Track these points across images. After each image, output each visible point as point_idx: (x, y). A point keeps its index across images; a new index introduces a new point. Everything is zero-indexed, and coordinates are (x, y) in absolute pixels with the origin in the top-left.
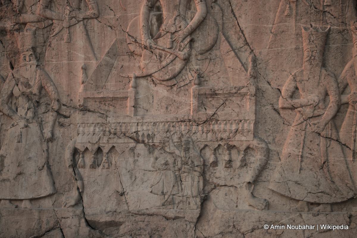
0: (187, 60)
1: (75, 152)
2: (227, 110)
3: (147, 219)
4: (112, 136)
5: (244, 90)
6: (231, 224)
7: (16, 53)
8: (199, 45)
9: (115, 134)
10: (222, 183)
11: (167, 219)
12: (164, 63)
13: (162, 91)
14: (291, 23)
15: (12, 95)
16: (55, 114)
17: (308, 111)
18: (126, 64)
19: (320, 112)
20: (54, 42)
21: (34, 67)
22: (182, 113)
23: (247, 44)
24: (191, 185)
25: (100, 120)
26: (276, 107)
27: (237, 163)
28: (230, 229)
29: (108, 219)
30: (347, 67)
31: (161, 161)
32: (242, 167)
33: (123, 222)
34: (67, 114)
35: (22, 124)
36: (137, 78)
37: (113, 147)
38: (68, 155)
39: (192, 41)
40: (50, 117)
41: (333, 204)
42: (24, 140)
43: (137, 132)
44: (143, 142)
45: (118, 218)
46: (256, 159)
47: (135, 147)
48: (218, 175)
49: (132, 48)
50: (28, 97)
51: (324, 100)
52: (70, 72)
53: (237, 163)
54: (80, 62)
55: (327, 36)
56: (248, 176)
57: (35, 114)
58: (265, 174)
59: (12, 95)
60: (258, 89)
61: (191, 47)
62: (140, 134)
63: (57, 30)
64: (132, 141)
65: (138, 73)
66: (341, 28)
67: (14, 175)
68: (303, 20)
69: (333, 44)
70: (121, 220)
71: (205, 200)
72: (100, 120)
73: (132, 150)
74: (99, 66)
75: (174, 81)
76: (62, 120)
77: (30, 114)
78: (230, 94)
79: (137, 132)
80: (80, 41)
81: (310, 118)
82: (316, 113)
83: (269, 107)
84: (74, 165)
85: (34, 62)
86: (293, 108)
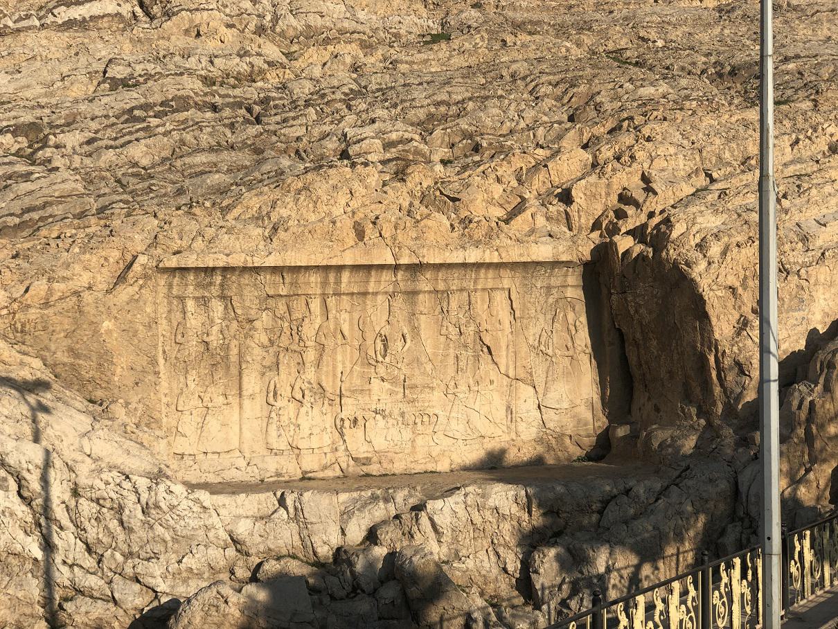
2: (423, 396)
14: (451, 351)
18: (366, 370)
21: (313, 372)
25: (355, 402)
31: (390, 424)
35: (309, 405)
45: (370, 455)
52: (334, 375)
54: (340, 369)
72: (356, 402)
76: (330, 402)
77: (312, 400)
78: (424, 387)
80: (339, 358)
85: (313, 369)
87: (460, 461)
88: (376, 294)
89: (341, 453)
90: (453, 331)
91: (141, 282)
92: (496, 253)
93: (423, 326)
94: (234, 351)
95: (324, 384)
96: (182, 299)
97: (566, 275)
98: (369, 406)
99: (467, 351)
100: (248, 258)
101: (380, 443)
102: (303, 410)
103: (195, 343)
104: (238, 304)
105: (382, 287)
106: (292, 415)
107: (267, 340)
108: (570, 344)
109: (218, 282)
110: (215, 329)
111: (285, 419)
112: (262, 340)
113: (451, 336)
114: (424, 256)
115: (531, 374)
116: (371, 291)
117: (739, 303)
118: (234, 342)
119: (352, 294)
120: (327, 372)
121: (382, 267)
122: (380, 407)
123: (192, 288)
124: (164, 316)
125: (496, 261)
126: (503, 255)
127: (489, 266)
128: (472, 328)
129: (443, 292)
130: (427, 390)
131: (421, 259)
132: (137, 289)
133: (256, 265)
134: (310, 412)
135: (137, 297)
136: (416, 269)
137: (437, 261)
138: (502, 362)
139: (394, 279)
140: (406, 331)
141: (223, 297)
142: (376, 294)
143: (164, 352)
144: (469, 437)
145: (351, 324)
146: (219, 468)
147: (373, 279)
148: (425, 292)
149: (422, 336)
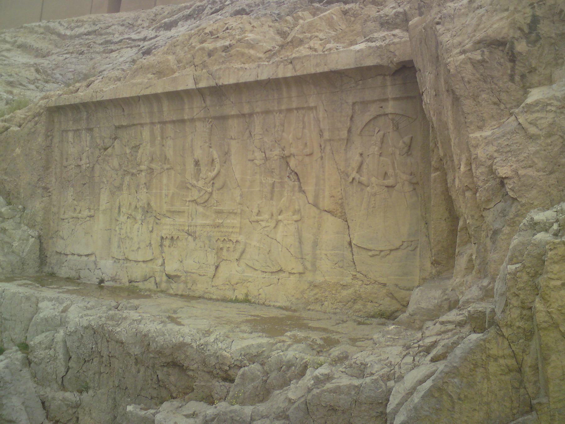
0: (211, 194)
1: (162, 238)
2: (229, 221)
3: (192, 275)
5: (235, 211)
7: (138, 186)
8: (217, 185)
11: (200, 275)
12: (201, 194)
13: (200, 209)
15: (136, 207)
17: (264, 224)
19: (269, 224)
20: (154, 180)
22: (208, 222)
23: (239, 186)
24: (212, 259)
25: (172, 223)
27: (232, 249)
28: (227, 283)
29: (175, 274)
30: (282, 201)
32: (233, 251)
35: (140, 222)
36: (189, 201)
38: (159, 239)
39: (213, 183)
40: (152, 220)
41: (272, 273)
42: (140, 231)
43: (188, 230)
44: (191, 235)
45: (179, 274)
46: (240, 248)
48: (224, 254)
51: (271, 218)
53: (232, 249)
55: (273, 185)
56: (237, 255)
57: (145, 217)
58: (244, 255)
59: (136, 207)
60: (242, 210)
61: (213, 186)
63: (155, 174)
65: (190, 198)
66: (280, 181)
67: (136, 249)
71: (217, 267)
73: (186, 239)
74: (173, 194)
75: (206, 204)
76: (157, 221)
77: (143, 217)
78: (230, 213)
79: (188, 230)
80: (165, 181)
82: (267, 224)
83: (247, 220)
84: (161, 246)
85: (145, 190)
87: (256, 293)
88: (192, 120)
89: (158, 268)
90: (258, 155)
91: (36, 119)
92: (290, 66)
94: (97, 174)
96: (67, 131)
97: (384, 86)
99: (273, 177)
100: (94, 94)
101: (190, 264)
102: (137, 226)
103: (73, 166)
104: (98, 135)
105: (195, 114)
106: (128, 230)
108: (390, 172)
109: (85, 117)
111: (123, 231)
113: (256, 161)
114: (220, 78)
115: (342, 205)
116: (186, 118)
117: (520, 68)
118: (97, 167)
119: (173, 122)
121: (187, 92)
122: (192, 229)
123: (71, 123)
124: (57, 145)
125: (289, 75)
126: (298, 67)
127: (286, 81)
128: (277, 151)
129: (251, 115)
131: (217, 81)
132: (33, 124)
133: (98, 99)
135: (33, 130)
136: (218, 92)
137: (232, 81)
138: (310, 189)
139: (204, 105)
140: (215, 156)
141: (90, 130)
142: (192, 120)
143: (56, 173)
144: (269, 270)
146: (79, 267)
147: (186, 107)
148: (233, 116)
149: (233, 161)
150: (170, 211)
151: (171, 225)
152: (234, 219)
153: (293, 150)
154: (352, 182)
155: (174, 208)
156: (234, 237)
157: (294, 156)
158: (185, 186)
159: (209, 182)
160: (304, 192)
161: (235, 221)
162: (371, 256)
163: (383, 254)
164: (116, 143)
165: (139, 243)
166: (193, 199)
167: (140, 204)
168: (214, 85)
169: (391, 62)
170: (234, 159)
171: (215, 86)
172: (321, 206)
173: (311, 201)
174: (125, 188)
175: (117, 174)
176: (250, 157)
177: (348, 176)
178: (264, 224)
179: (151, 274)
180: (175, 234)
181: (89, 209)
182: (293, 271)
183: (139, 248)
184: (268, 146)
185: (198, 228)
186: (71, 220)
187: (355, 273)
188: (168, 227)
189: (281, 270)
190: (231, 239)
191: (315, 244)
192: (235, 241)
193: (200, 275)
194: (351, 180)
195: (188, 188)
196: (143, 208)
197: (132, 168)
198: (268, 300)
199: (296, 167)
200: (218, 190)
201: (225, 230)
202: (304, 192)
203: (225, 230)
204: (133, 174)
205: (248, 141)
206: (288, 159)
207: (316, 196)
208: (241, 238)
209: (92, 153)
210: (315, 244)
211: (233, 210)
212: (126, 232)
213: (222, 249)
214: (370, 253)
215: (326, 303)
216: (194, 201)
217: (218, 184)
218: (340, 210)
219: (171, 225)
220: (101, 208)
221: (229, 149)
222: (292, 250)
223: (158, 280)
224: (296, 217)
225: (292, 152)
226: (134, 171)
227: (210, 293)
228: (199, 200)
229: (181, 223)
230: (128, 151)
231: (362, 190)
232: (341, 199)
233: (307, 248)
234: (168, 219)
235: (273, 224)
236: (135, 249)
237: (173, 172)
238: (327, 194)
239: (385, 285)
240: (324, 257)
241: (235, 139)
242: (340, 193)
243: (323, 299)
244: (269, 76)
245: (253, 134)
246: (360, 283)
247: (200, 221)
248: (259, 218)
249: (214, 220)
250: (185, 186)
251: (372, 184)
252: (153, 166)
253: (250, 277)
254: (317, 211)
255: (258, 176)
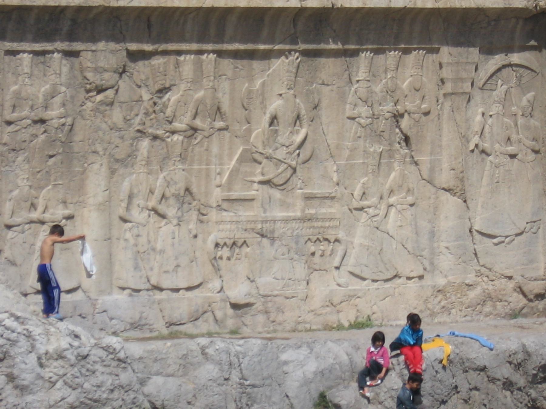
2: (323, 210)
4: (243, 232)
5: (333, 195)
6: (328, 300)
9: (246, 230)
10: (318, 268)
11: (287, 298)
12: (280, 170)
13: (277, 194)
15: (163, 196)
16: (197, 213)
20: (197, 149)
23: (332, 156)
25: (235, 219)
26: (351, 207)
28: (327, 303)
33: (255, 303)
34: (204, 212)
35: (175, 222)
37: (245, 242)
40: (194, 215)
41: (387, 280)
44: (266, 236)
45: (252, 300)
47: (261, 241)
49: (257, 156)
50: (177, 196)
62: (264, 230)
64: (258, 236)
65: (261, 178)
68: (368, 141)
69: (384, 160)
70: (255, 301)
73: (259, 243)
76: (201, 217)
77: (180, 214)
80: (215, 149)
81: (373, 217)
82: (377, 212)
83: (346, 207)
86: (361, 209)
93: (324, 103)
95: (194, 190)
98: (252, 226)
101: (266, 281)
103: (29, 121)
107: (121, 119)
108: (514, 137)
110: (58, 100)
111: (143, 240)
112: (115, 119)
113: (362, 121)
115: (462, 180)
118: (80, 124)
120: (200, 171)
128: (389, 107)
130: (328, 202)
134: (177, 233)
139: (292, 31)
145: (232, 99)
149: (324, 119)
150: (228, 200)
151: (231, 222)
152: (330, 207)
153: (409, 106)
154: (473, 151)
155: (235, 195)
156: (331, 235)
157: (409, 114)
158: (250, 158)
159: (294, 151)
160: (416, 163)
161: (333, 210)
162: (496, 244)
163: (508, 240)
164: (124, 84)
165: (176, 258)
166: (266, 178)
167: (173, 190)
168: (331, 6)
169: (536, 6)
170: (325, 114)
171: (329, 8)
172: (437, 182)
173: (425, 177)
174: (143, 163)
175: (122, 138)
176: (349, 113)
177: (468, 141)
178: (371, 211)
179: (206, 307)
180: (240, 236)
181: (64, 202)
182: (412, 275)
183: (178, 266)
184: (377, 98)
185: (278, 224)
186: (27, 226)
187: (479, 268)
188: (228, 226)
189: (395, 276)
190: (327, 237)
191: (432, 234)
192: (332, 240)
193: (287, 298)
194: (472, 147)
195: (255, 161)
196: (177, 196)
197: (151, 127)
198: (386, 320)
199: (410, 128)
200: (304, 162)
201: (320, 224)
202: (416, 163)
203: (320, 224)
204: (155, 138)
205: (347, 88)
206: (400, 120)
207: (432, 170)
208: (341, 235)
209: (72, 97)
210: (432, 234)
211: (331, 193)
212: (149, 242)
213: (313, 254)
214: (496, 241)
215: (453, 311)
216: (267, 182)
217: (305, 153)
218: (460, 187)
219: (231, 222)
220: (91, 201)
221: (319, 101)
222: (409, 246)
223: (219, 314)
224: (410, 199)
225: (408, 108)
226: (160, 132)
227: (305, 322)
228: (275, 181)
229: (249, 219)
230: (146, 96)
231: (483, 160)
232: (462, 172)
233: (424, 240)
234: (225, 214)
235: (382, 213)
236: (171, 268)
237: (227, 134)
238: (445, 165)
239: (510, 278)
240: (444, 251)
241: (328, 85)
242: (461, 164)
243: (450, 306)
244: (406, 5)
245: (354, 79)
246: (485, 279)
247: (280, 214)
248: (365, 203)
249: (303, 211)
250: (250, 158)
251: (496, 152)
252: (198, 123)
253: (360, 290)
254: (433, 190)
255: (361, 142)
